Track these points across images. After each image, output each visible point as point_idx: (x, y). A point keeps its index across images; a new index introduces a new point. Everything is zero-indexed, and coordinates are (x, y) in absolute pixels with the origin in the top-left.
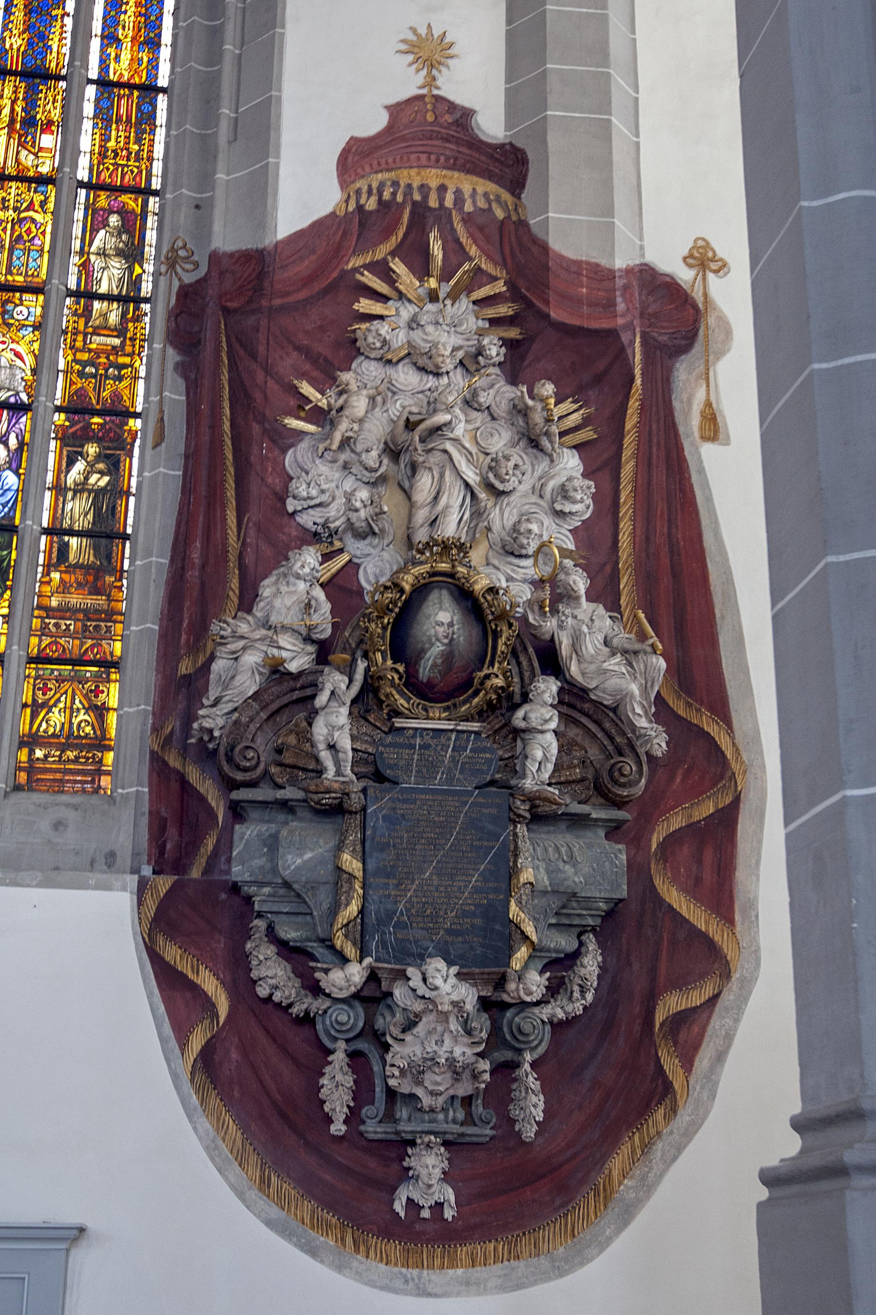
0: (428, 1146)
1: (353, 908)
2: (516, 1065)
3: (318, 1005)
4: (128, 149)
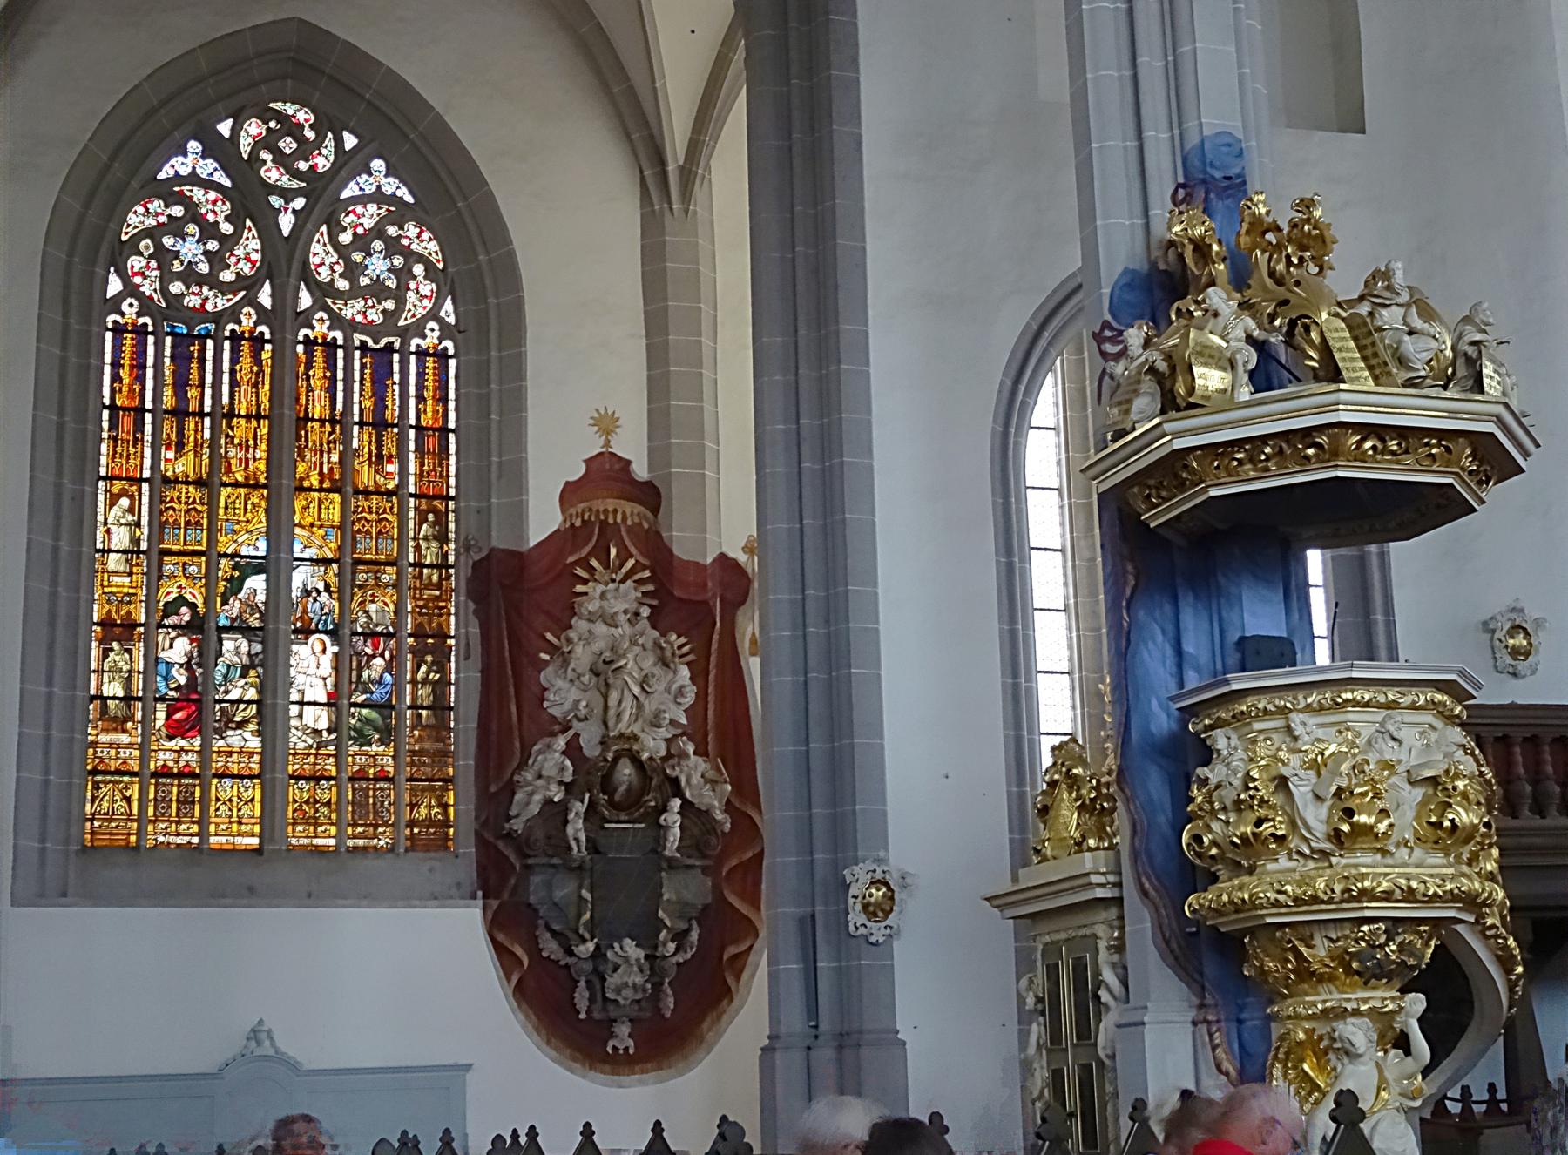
0: (623, 1023)
1: (587, 916)
2: (662, 984)
3: (571, 960)
4: (434, 470)
